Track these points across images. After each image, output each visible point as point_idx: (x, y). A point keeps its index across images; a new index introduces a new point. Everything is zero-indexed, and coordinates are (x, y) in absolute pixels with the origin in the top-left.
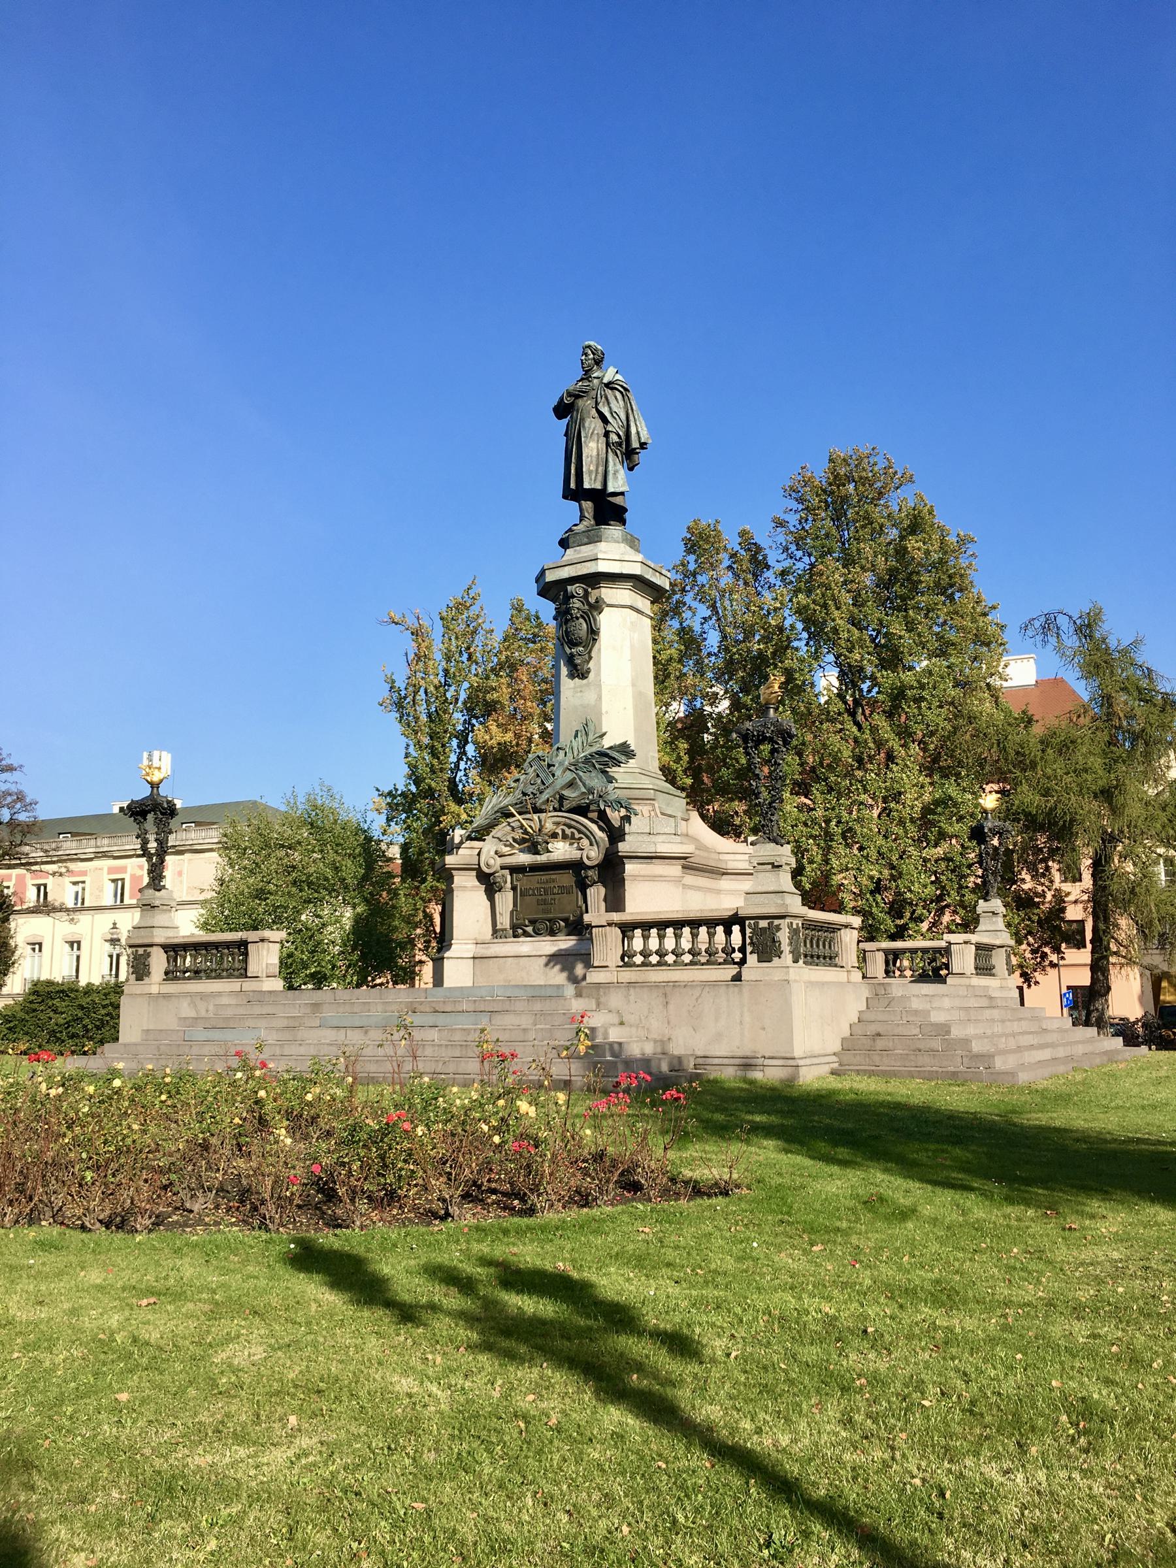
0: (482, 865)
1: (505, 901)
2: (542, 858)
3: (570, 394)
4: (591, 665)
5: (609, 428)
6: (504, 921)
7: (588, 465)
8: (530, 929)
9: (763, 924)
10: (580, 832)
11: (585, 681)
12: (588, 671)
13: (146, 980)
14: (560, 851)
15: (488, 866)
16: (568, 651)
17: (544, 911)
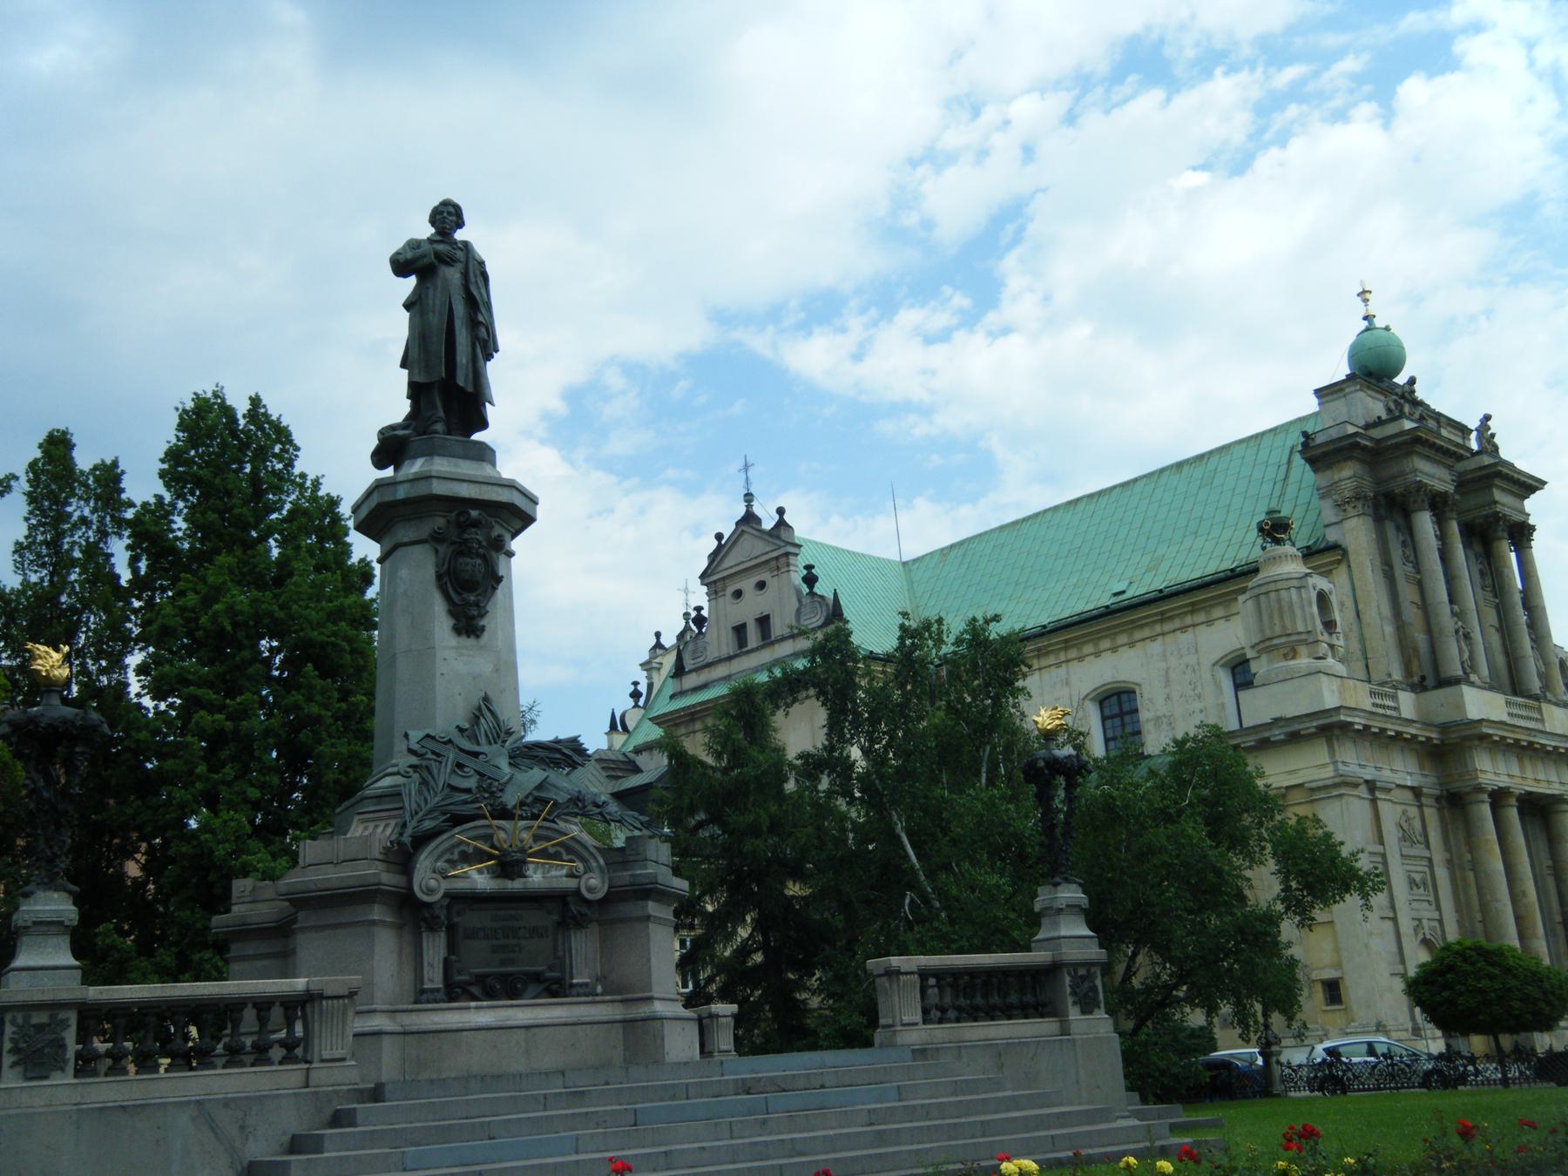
0: (416, 889)
1: (435, 949)
2: (516, 885)
3: (437, 255)
4: (483, 622)
5: (481, 318)
6: (434, 977)
7: (462, 357)
8: (475, 990)
9: (1082, 972)
10: (569, 850)
11: (471, 641)
12: (483, 629)
13: (57, 1079)
14: (537, 877)
15: (430, 891)
16: (456, 598)
17: (503, 963)
